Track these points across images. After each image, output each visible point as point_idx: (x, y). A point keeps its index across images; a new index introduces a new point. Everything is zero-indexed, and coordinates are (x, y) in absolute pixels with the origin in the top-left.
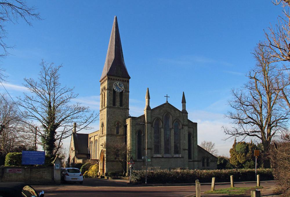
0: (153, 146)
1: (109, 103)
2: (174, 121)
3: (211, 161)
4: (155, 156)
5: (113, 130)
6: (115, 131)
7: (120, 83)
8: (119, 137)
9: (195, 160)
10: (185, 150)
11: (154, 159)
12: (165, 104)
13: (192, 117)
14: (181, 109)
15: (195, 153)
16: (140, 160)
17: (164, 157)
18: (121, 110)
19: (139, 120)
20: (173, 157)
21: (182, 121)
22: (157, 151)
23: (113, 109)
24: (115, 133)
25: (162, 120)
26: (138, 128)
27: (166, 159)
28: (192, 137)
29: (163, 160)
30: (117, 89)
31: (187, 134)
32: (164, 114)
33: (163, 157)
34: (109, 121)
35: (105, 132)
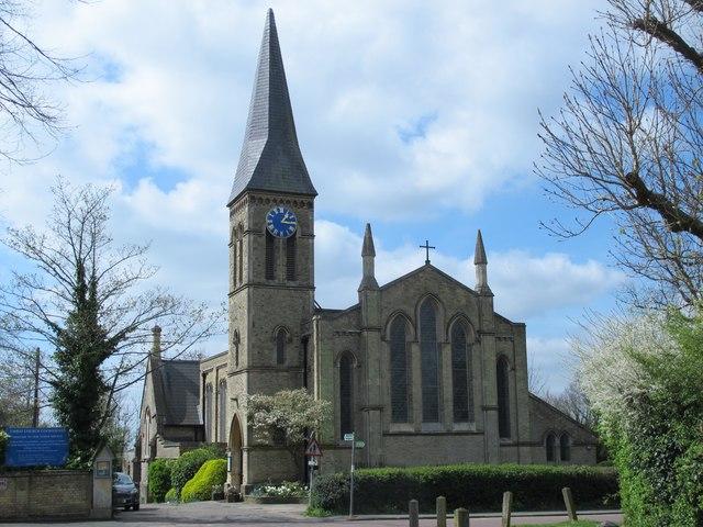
0: (387, 400)
3: (576, 444)
4: (395, 428)
5: (266, 352)
6: (275, 355)
8: (285, 374)
12: (421, 270)
15: (520, 420)
17: (423, 431)
19: (344, 320)
20: (449, 433)
21: (475, 320)
22: (400, 411)
24: (274, 362)
26: (342, 344)
27: (430, 438)
35: (244, 359)
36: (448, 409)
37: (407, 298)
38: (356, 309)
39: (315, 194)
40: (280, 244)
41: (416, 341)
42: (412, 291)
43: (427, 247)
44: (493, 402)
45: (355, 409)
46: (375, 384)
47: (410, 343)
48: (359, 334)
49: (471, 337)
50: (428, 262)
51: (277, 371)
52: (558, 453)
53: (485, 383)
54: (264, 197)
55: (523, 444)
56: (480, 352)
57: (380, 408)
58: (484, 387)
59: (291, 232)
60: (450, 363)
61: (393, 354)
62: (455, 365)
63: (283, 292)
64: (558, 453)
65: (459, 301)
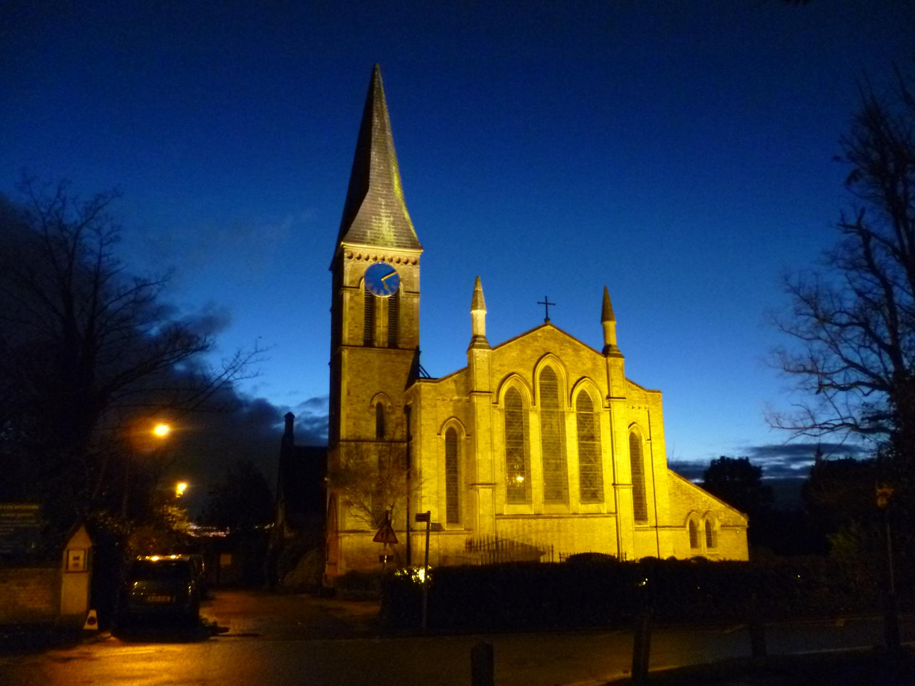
5: (363, 423)
6: (373, 426)
34: (349, 394)
37: (523, 360)
42: (529, 352)
43: (546, 304)
52: (702, 540)
57: (492, 485)
61: (509, 424)
62: (581, 438)
64: (702, 540)
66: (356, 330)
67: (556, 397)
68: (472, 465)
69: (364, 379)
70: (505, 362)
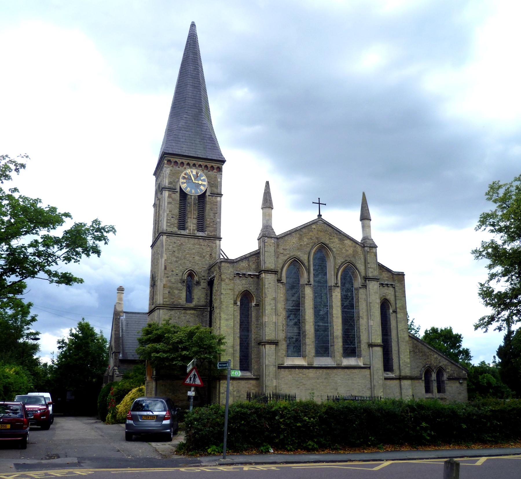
1: (167, 222)
2: (340, 267)
3: (449, 379)
4: (290, 362)
5: (176, 292)
6: (184, 295)
7: (197, 173)
9: (403, 374)
10: (371, 345)
11: (287, 370)
12: (314, 222)
13: (386, 257)
14: (358, 237)
15: (401, 356)
16: (248, 374)
17: (315, 364)
18: (201, 241)
19: (244, 264)
20: (339, 367)
23: (179, 238)
24: (182, 301)
25: (306, 264)
26: (241, 285)
27: (321, 371)
28: (391, 311)
29: (311, 373)
30: (188, 189)
31: (378, 301)
32: (311, 249)
33: (310, 367)
34: (165, 269)
36: (338, 344)
37: (301, 245)
38: (256, 254)
39: (223, 161)
40: (191, 201)
41: (309, 284)
42: (305, 239)
43: (319, 204)
44: (379, 340)
45: (253, 344)
46: (273, 320)
47: (303, 286)
48: (258, 277)
49: (358, 282)
50: (320, 216)
51: (186, 309)
52: (434, 386)
53: (371, 323)
54: (179, 161)
55: (406, 378)
56: (366, 295)
57: (275, 343)
58: (370, 327)
59: (201, 190)
60: (339, 304)
62: (343, 307)
63: (192, 241)
64: (434, 386)
65: (347, 251)
66: (172, 220)
67: (325, 274)
68: (261, 326)
69: (177, 257)
70: (288, 247)
